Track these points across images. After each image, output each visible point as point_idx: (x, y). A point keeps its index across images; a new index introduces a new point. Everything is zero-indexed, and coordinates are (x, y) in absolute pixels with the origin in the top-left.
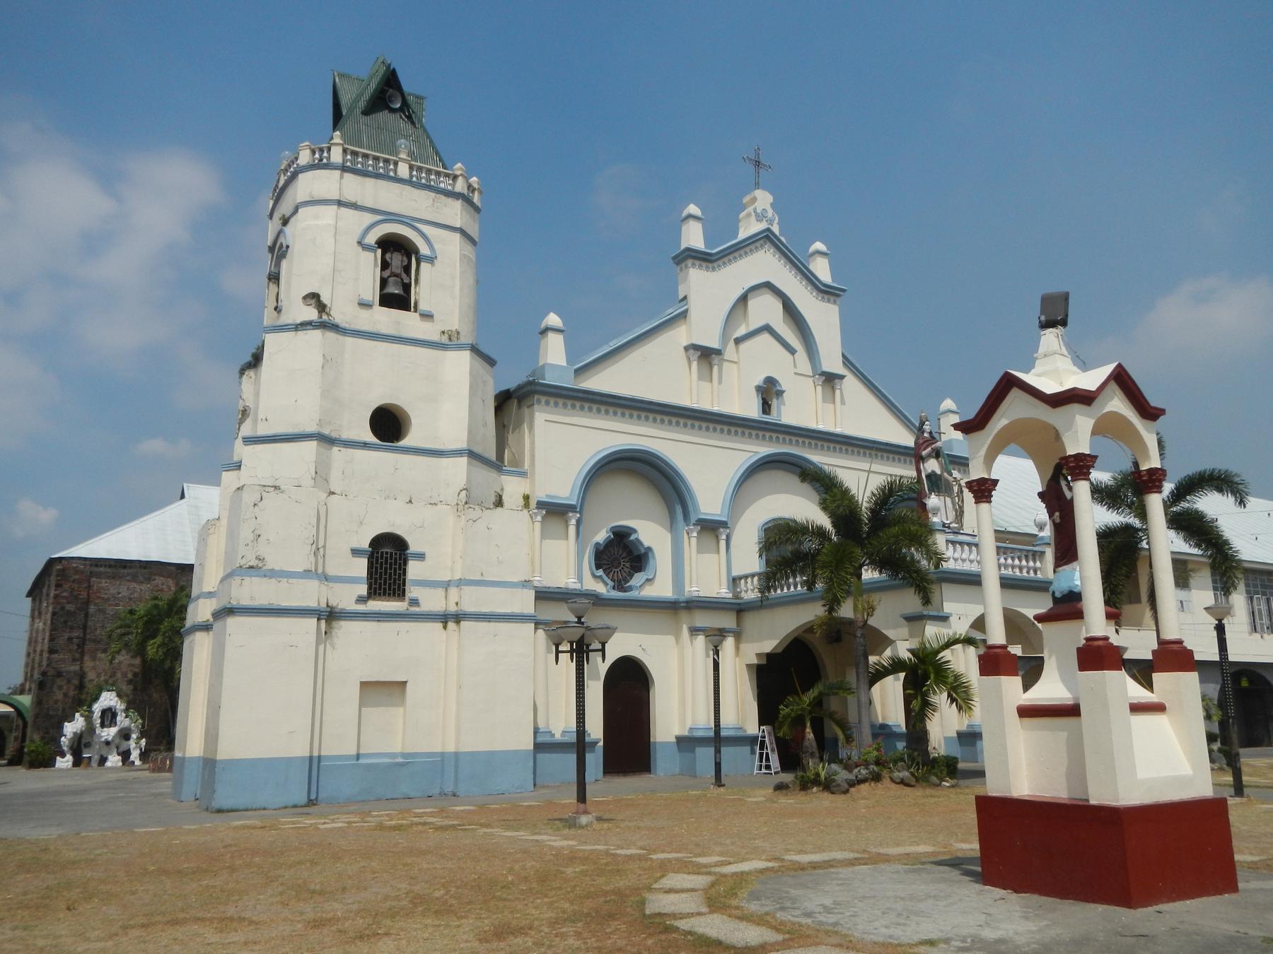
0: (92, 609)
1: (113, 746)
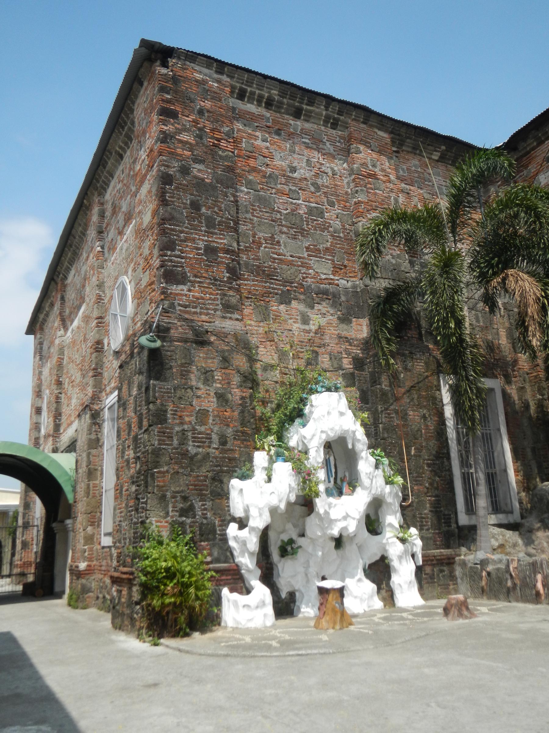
0: (244, 194)
1: (350, 549)
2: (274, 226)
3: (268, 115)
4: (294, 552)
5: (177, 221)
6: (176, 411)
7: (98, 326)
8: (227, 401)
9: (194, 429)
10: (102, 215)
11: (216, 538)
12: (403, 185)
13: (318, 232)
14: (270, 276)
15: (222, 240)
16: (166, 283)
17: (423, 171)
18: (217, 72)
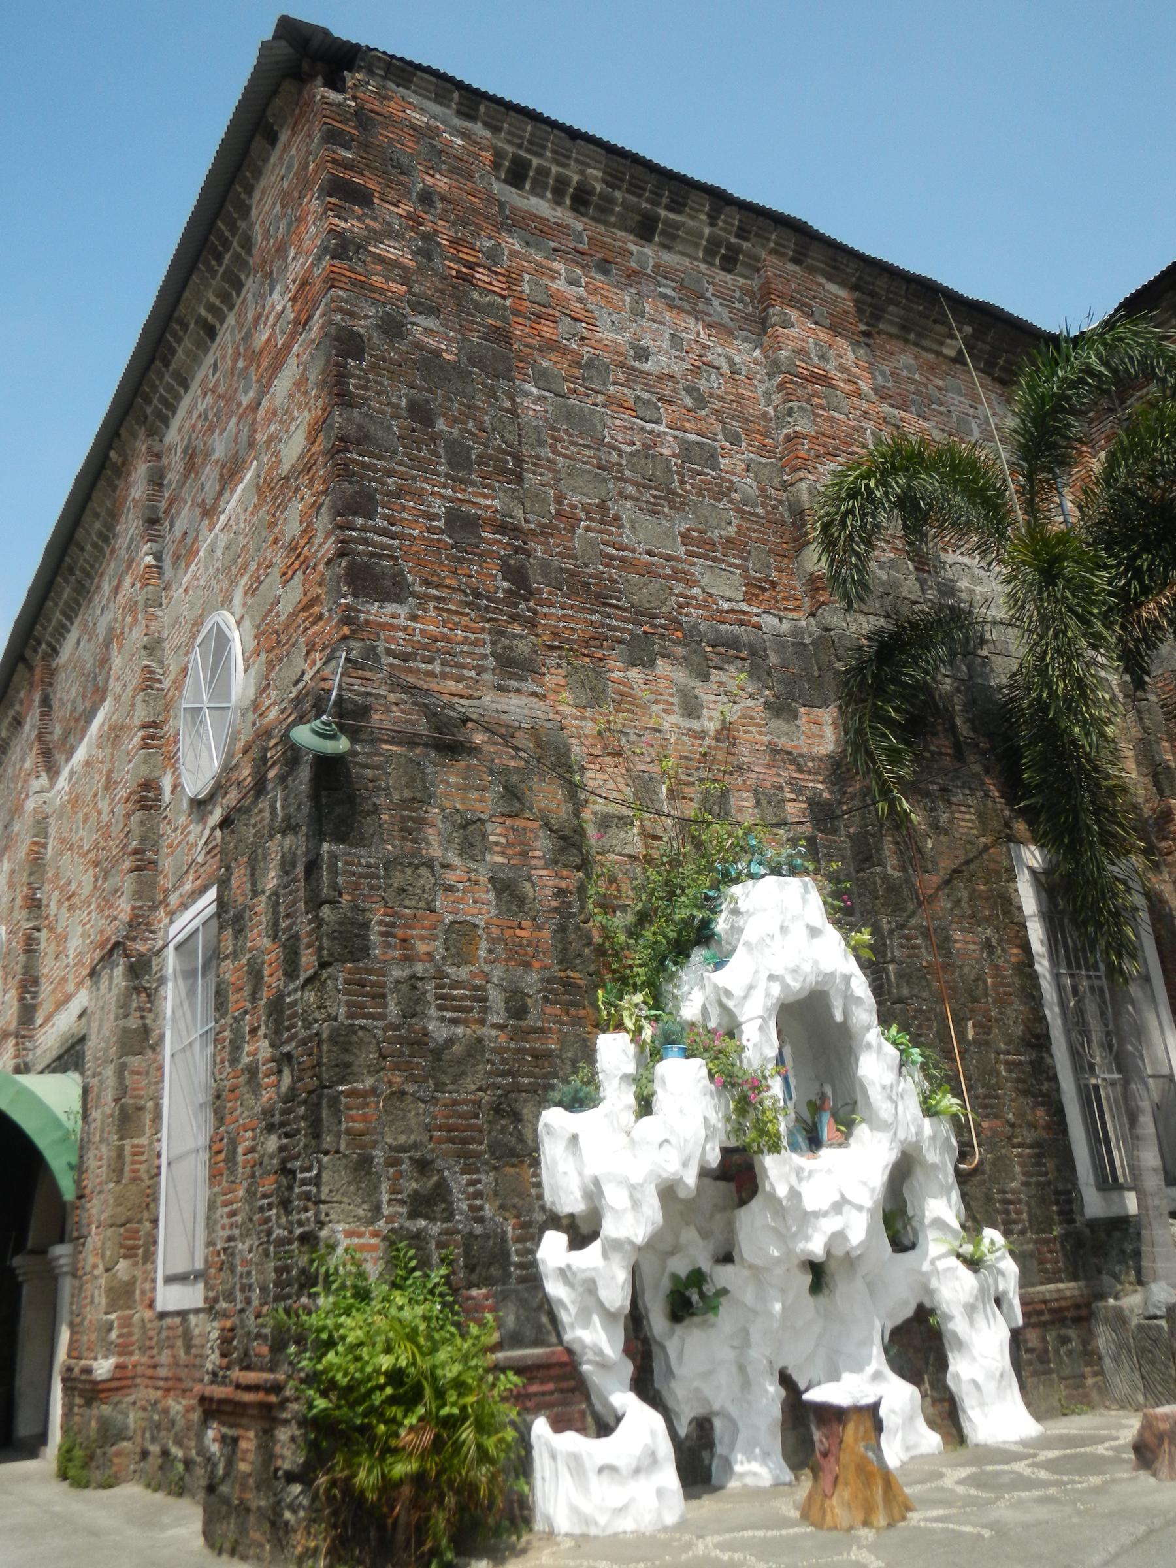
1: (847, 1292)
2: (605, 481)
3: (579, 226)
4: (711, 1304)
5: (378, 446)
6: (392, 925)
7: (146, 746)
8: (521, 900)
9: (441, 975)
10: (157, 480)
11: (509, 1275)
12: (886, 408)
13: (707, 501)
14: (600, 596)
15: (489, 501)
16: (355, 596)
17: (924, 380)
18: (459, 113)
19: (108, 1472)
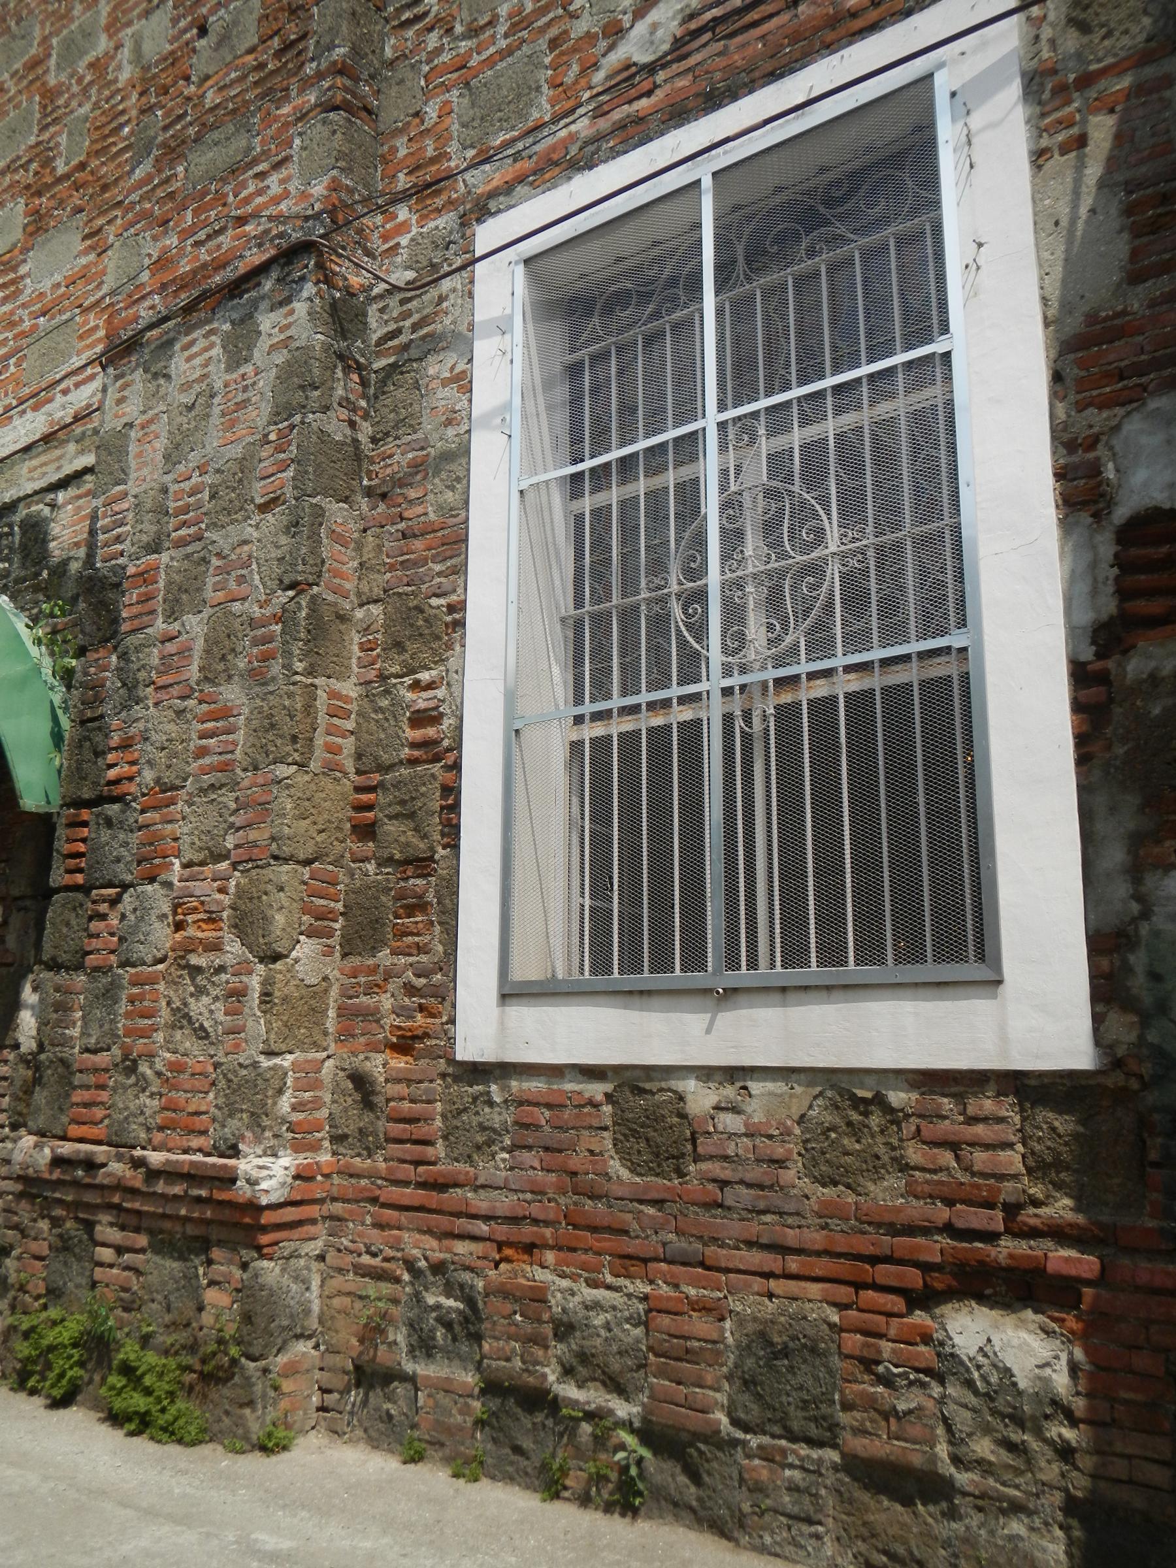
19: (272, 1414)
